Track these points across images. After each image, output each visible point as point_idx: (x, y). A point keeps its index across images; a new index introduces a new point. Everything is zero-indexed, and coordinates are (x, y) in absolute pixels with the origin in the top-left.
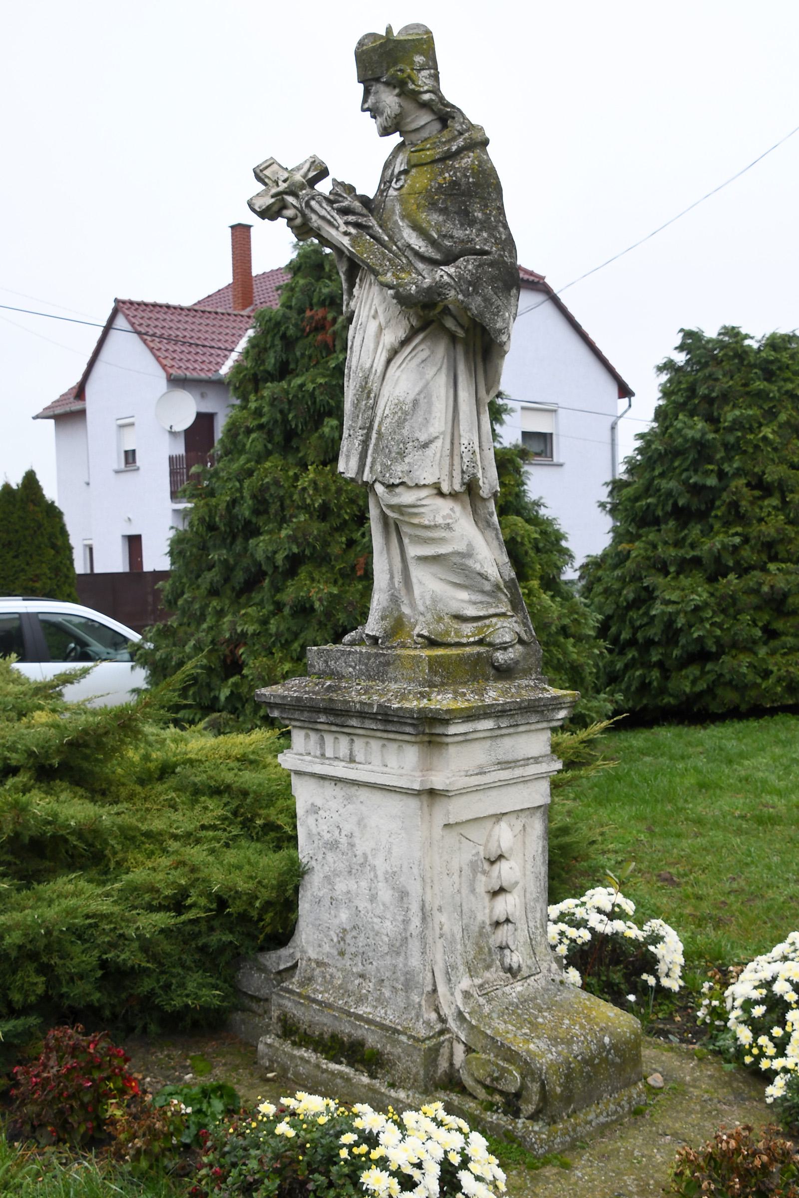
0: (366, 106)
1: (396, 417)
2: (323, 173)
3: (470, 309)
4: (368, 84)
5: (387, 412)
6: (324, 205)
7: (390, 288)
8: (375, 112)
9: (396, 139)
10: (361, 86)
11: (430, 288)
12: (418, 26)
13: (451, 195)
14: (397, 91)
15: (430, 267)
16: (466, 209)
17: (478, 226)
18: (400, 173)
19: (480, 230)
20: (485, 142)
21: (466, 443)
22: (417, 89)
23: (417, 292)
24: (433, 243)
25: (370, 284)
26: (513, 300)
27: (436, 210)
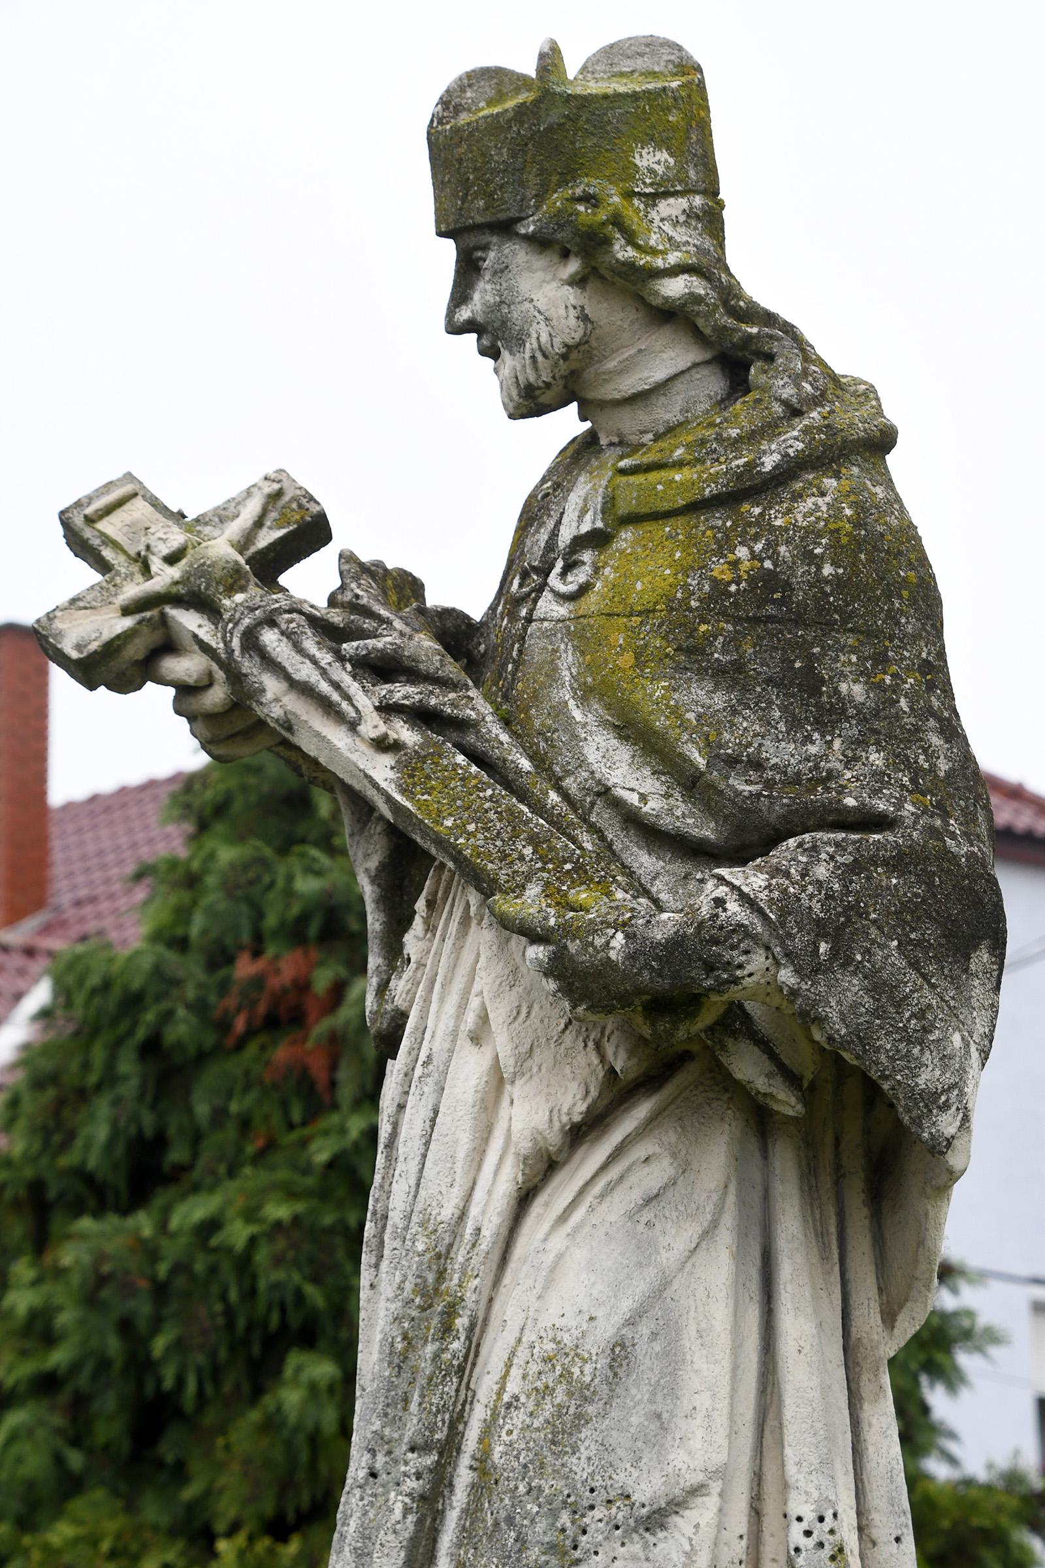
0: (464, 314)
1: (548, 1409)
2: (312, 533)
3: (820, 1020)
4: (472, 240)
5: (513, 1387)
6: (310, 645)
7: (535, 938)
8: (494, 336)
9: (565, 424)
10: (449, 247)
11: (676, 943)
12: (652, 45)
13: (756, 621)
14: (573, 266)
15: (680, 868)
16: (809, 670)
17: (852, 730)
18: (580, 542)
19: (861, 742)
20: (883, 441)
21: (810, 1515)
22: (643, 260)
23: (631, 957)
24: (690, 783)
25: (465, 921)
26: (978, 990)
27: (701, 673)
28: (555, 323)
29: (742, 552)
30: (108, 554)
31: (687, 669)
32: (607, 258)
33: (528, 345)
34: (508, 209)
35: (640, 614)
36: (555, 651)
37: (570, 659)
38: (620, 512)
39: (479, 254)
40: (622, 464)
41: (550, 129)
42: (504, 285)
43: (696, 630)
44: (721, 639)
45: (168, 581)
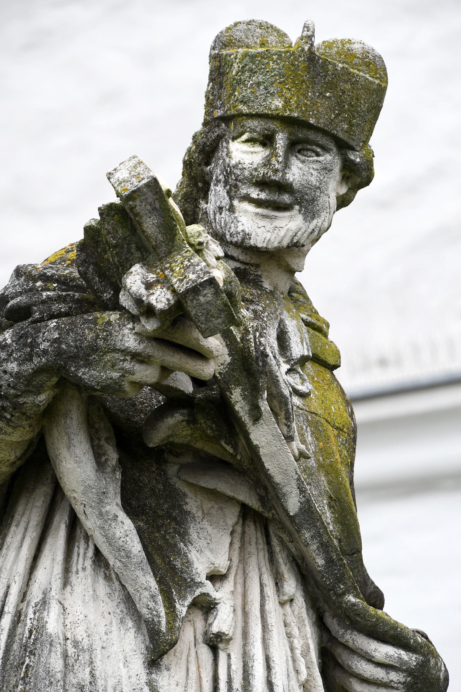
33: (315, 222)
39: (319, 150)
42: (325, 179)
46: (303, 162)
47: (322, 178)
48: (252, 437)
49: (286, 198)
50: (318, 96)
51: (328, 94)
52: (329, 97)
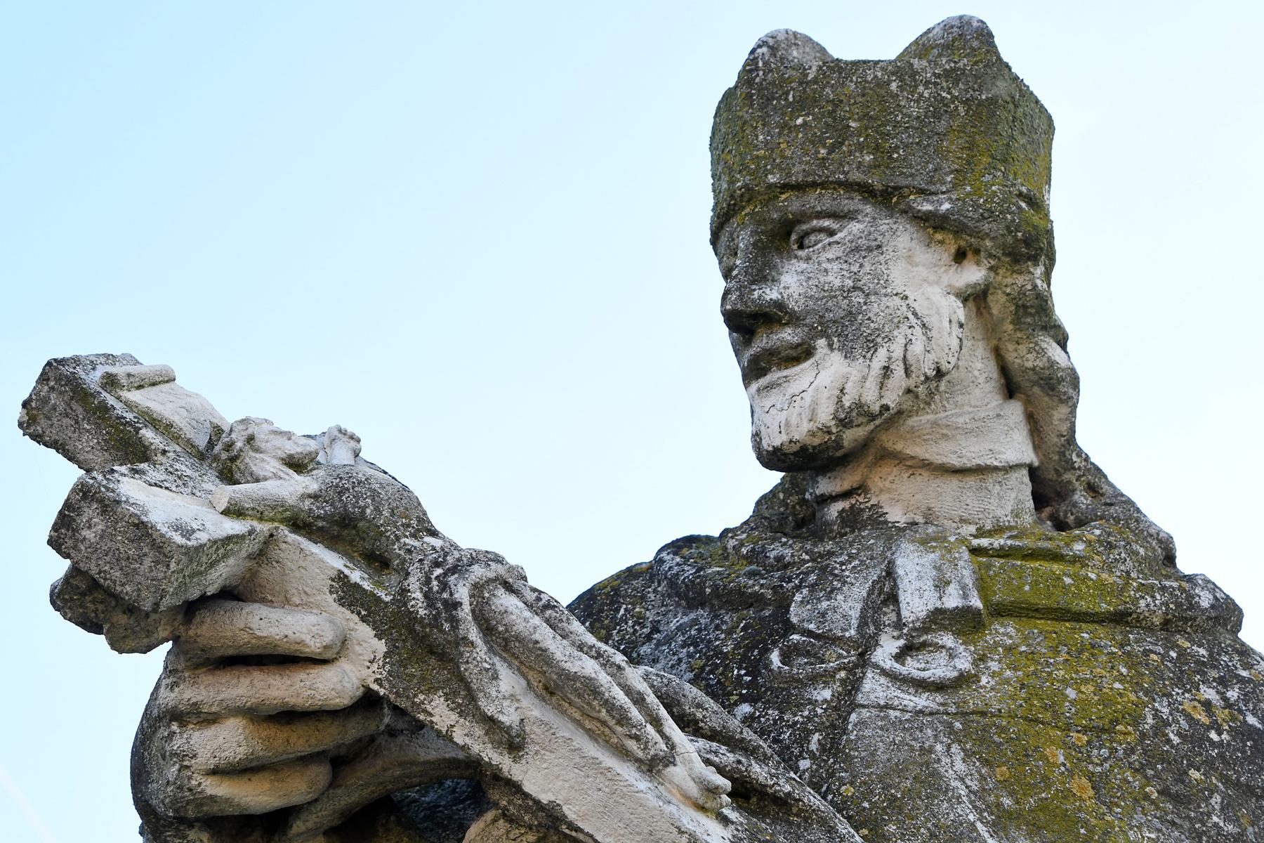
14: (973, 274)
18: (938, 619)
28: (934, 333)
29: (1209, 693)
30: (148, 434)
31: (1173, 823)
32: (1020, 280)
33: (882, 354)
34: (912, 175)
35: (1085, 730)
36: (931, 750)
37: (960, 766)
38: (997, 598)
39: (826, 223)
40: (984, 542)
41: (992, 101)
42: (867, 268)
43: (1186, 773)
44: (1216, 799)
45: (301, 491)
46: (808, 259)
47: (855, 268)
48: (528, 787)
49: (788, 335)
50: (780, 134)
51: (800, 121)
52: (805, 123)
